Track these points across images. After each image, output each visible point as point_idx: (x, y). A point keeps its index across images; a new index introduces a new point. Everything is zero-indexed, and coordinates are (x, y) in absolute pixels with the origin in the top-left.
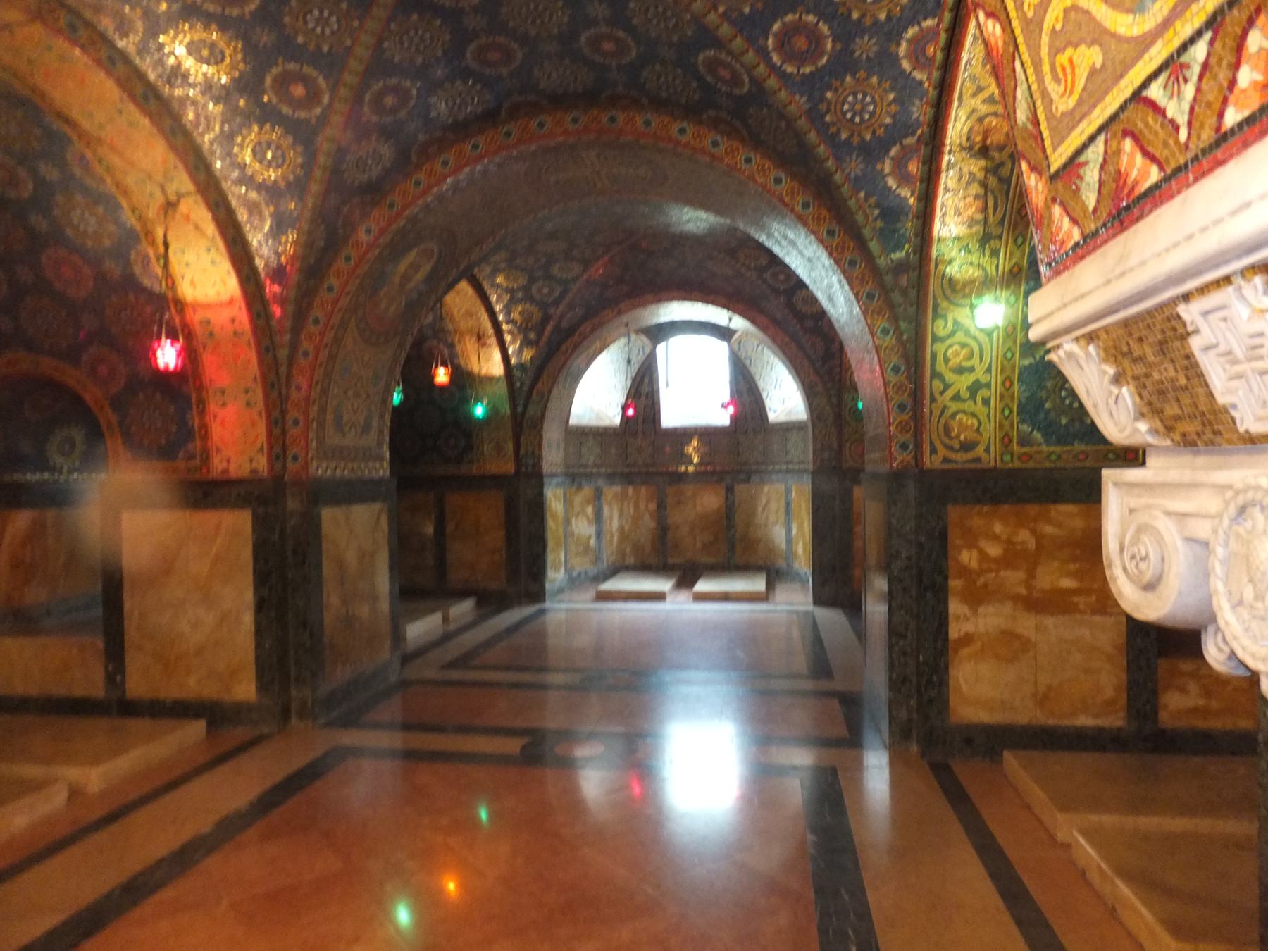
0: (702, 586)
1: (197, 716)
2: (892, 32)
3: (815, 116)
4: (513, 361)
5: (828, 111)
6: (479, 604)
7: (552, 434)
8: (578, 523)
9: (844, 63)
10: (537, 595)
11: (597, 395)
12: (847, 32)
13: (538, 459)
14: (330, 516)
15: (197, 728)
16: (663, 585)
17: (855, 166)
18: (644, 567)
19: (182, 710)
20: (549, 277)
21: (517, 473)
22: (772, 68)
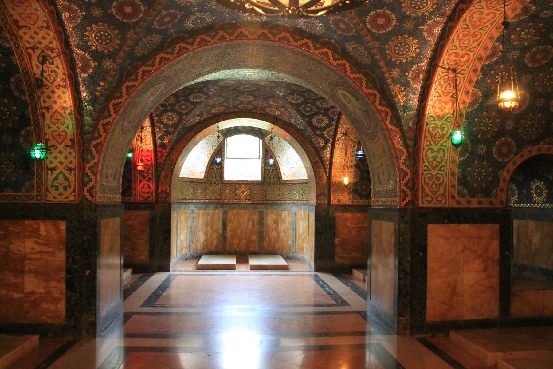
0: (253, 262)
1: (34, 333)
2: (423, 20)
3: (382, 51)
4: (158, 142)
5: (389, 49)
6: (134, 273)
7: (174, 182)
8: (187, 229)
9: (398, 32)
10: (165, 268)
11: (194, 163)
12: (402, 18)
13: (168, 195)
14: (375, 224)
15: (35, 339)
16: (232, 261)
17: (395, 73)
18: (212, 253)
19: (24, 329)
20: (187, 100)
21: (157, 201)
22: (369, 31)
